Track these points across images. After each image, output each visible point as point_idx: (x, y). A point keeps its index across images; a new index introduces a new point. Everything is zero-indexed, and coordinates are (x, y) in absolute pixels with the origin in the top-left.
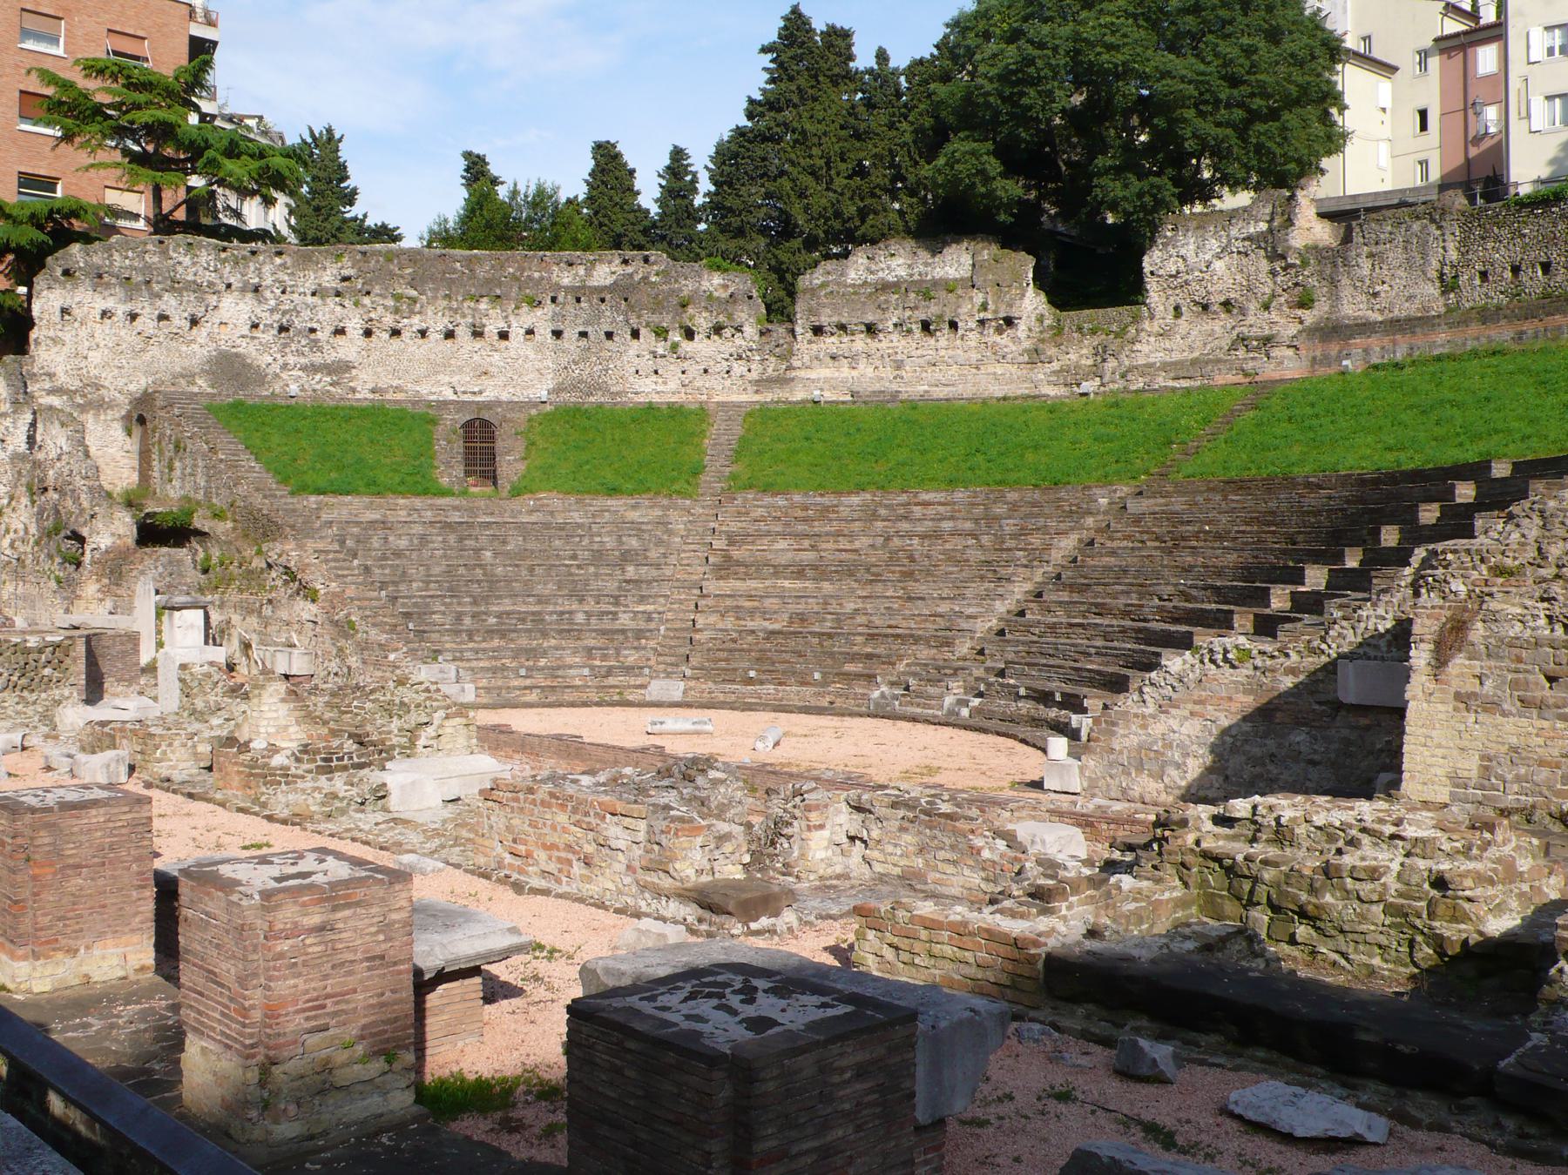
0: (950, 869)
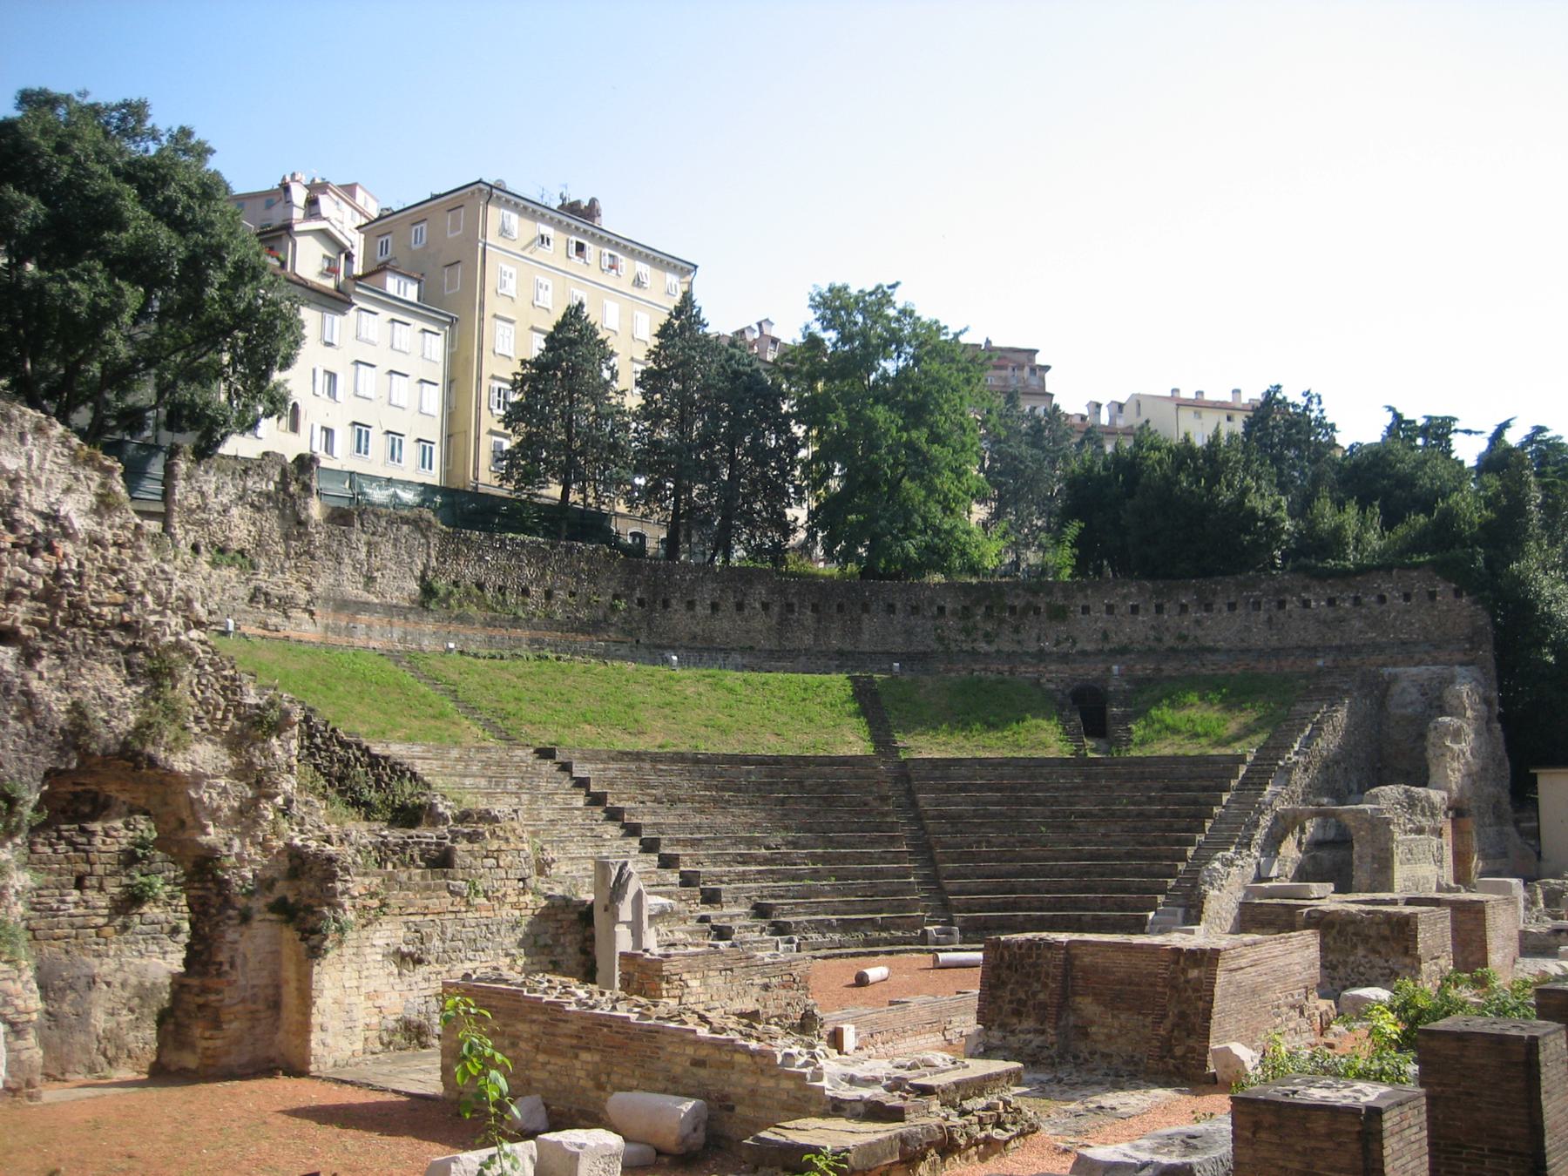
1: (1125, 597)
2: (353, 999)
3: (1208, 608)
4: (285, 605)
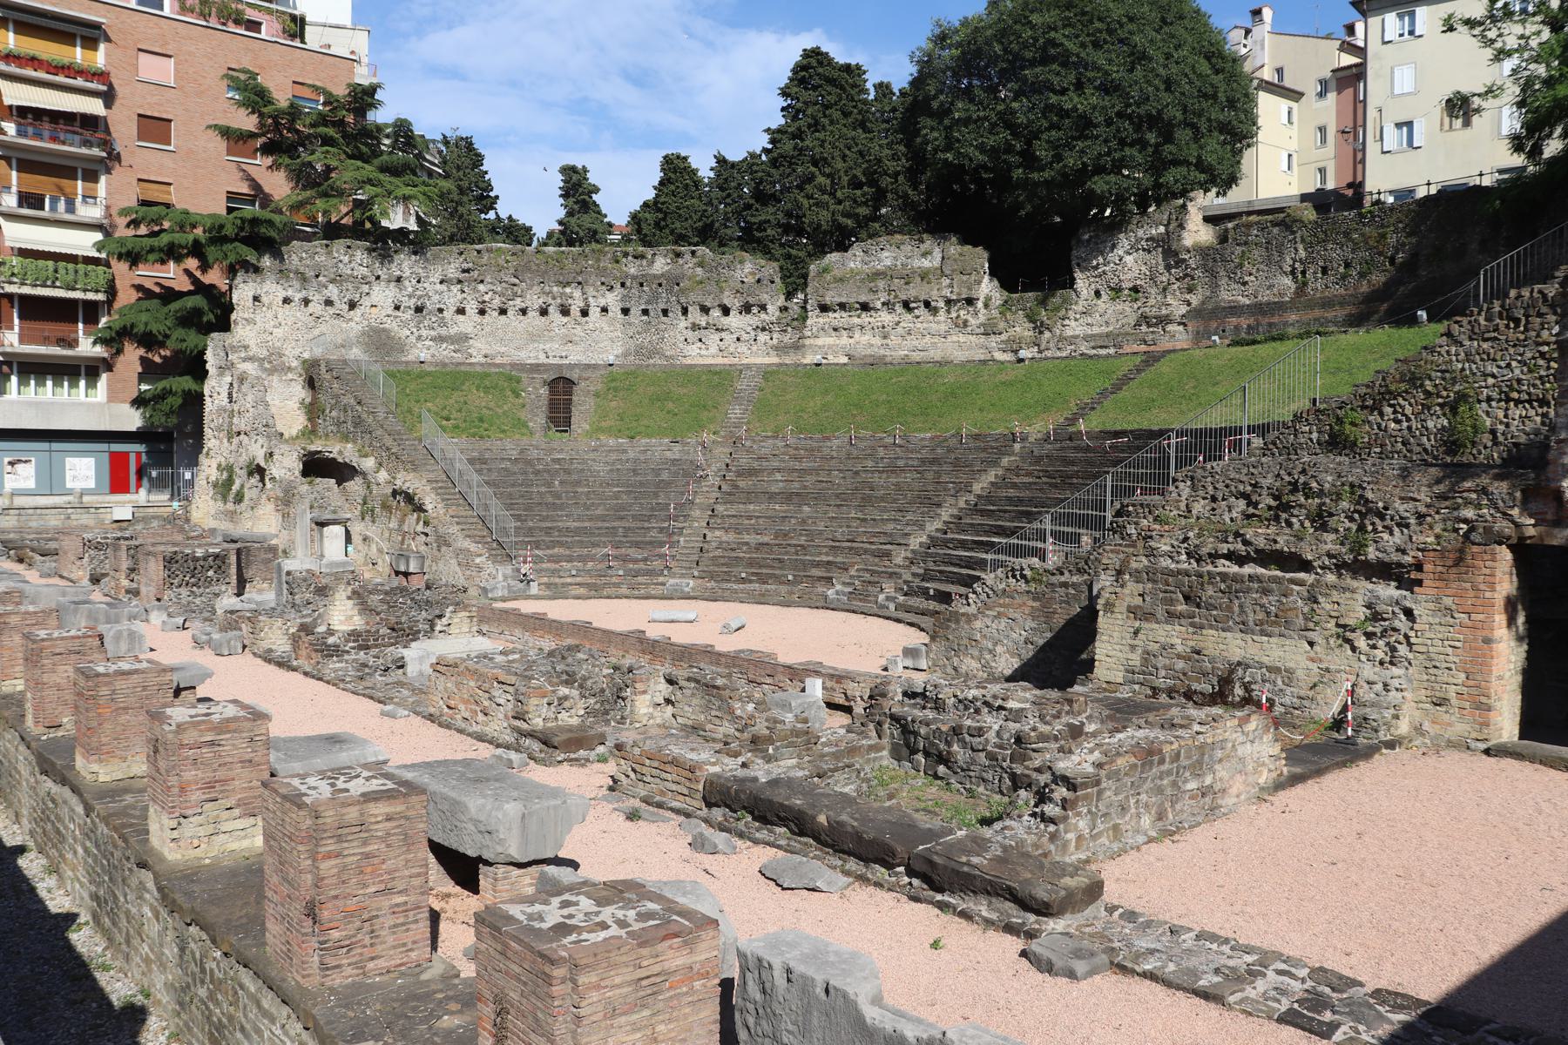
0: (717, 722)
4: (1164, 321)
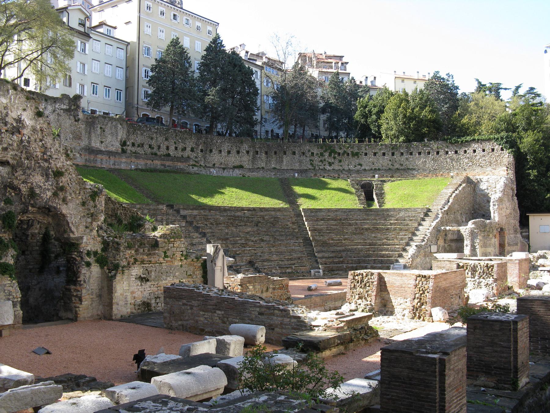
1: (380, 149)
2: (127, 294)
3: (411, 154)
